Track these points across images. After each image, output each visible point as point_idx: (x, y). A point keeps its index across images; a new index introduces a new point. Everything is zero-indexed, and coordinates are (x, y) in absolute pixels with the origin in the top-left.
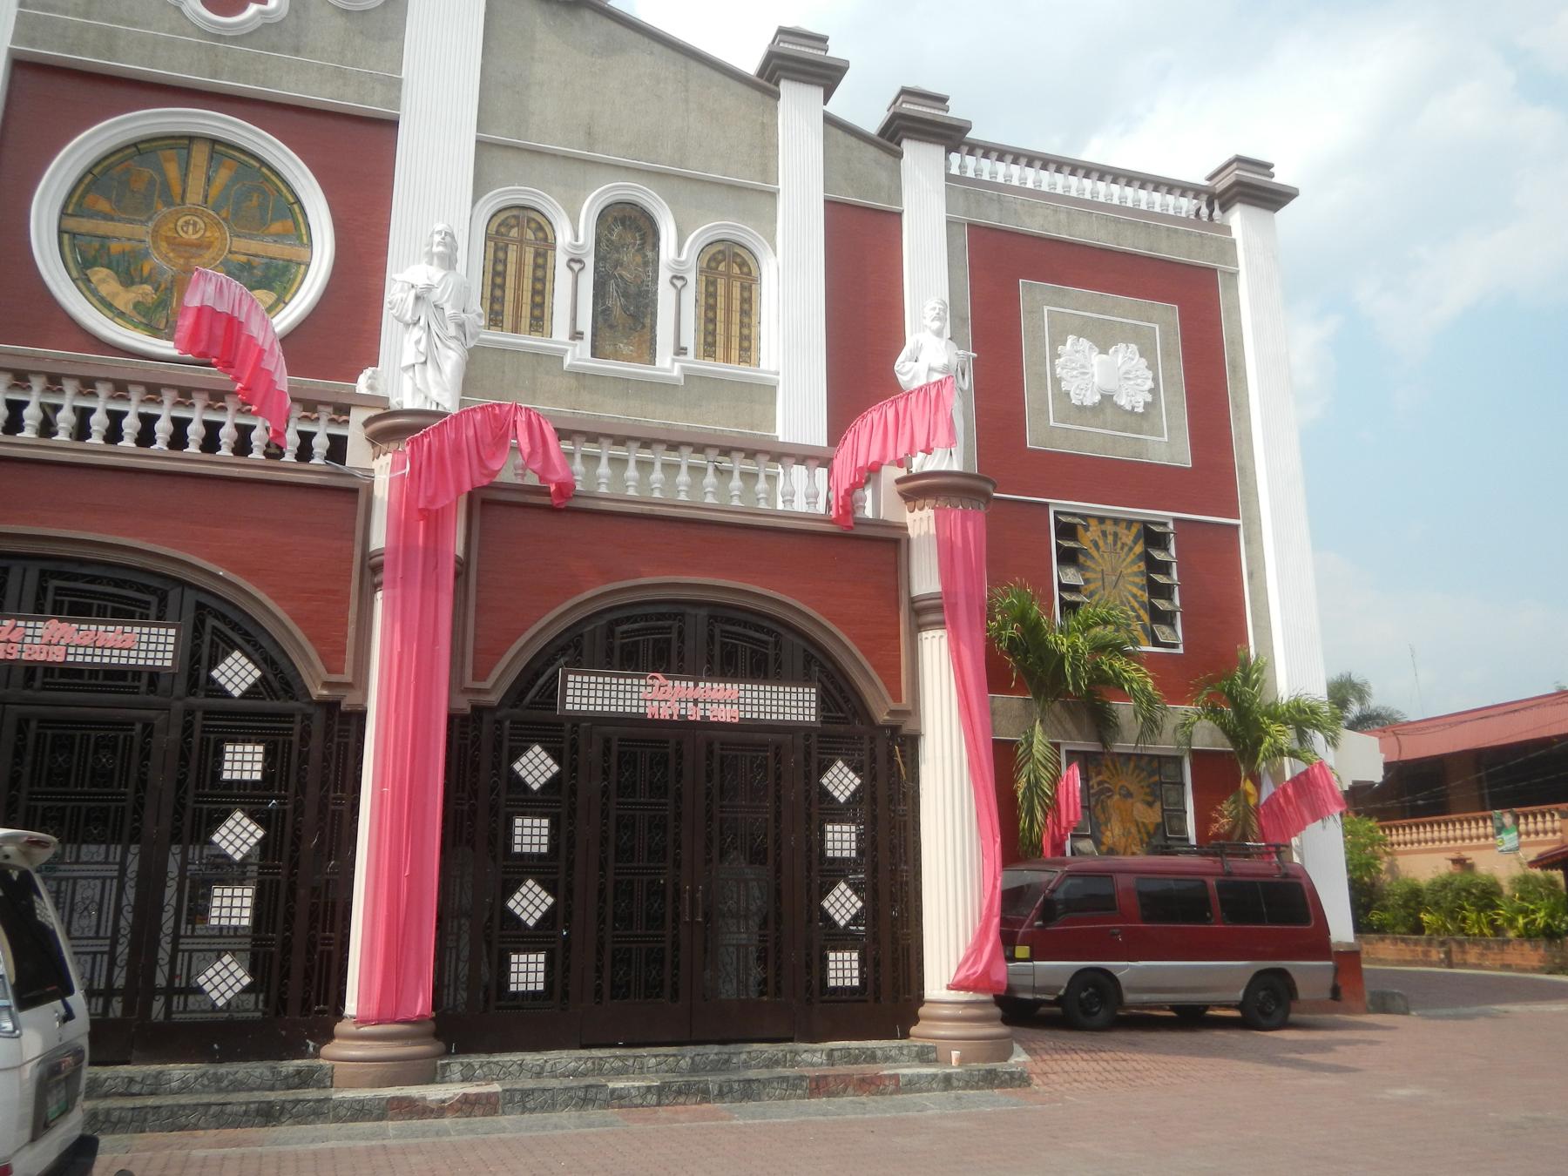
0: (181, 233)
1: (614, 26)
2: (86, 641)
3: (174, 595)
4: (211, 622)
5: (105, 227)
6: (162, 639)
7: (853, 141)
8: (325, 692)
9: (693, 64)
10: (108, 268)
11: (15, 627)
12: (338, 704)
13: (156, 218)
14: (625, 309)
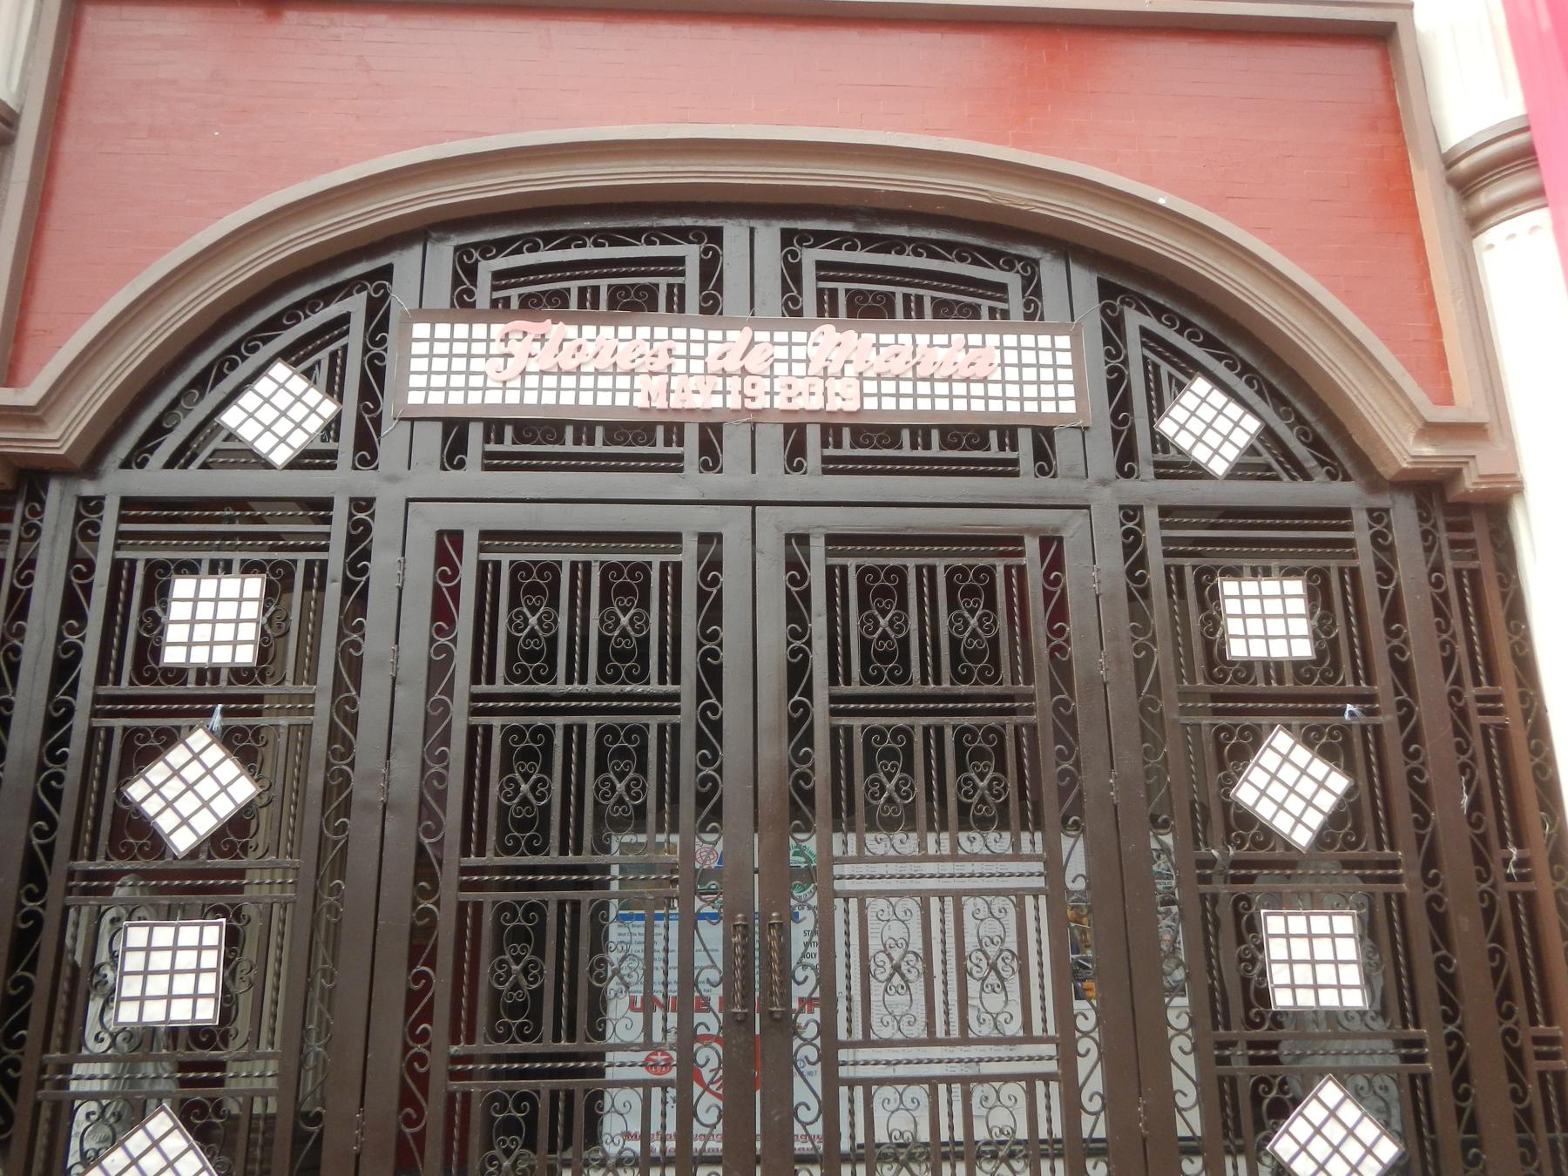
2: (898, 367)
3: (1051, 271)
4: (1134, 320)
6: (1046, 358)
8: (1427, 450)
11: (752, 343)
12: (1455, 475)
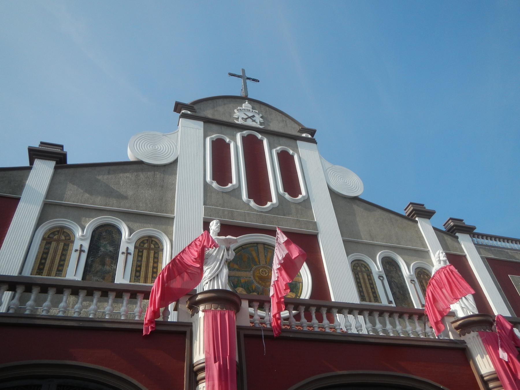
0: (262, 274)
1: (367, 205)
5: (238, 274)
7: (442, 234)
9: (392, 216)
10: (241, 287)
13: (253, 269)
14: (400, 292)
